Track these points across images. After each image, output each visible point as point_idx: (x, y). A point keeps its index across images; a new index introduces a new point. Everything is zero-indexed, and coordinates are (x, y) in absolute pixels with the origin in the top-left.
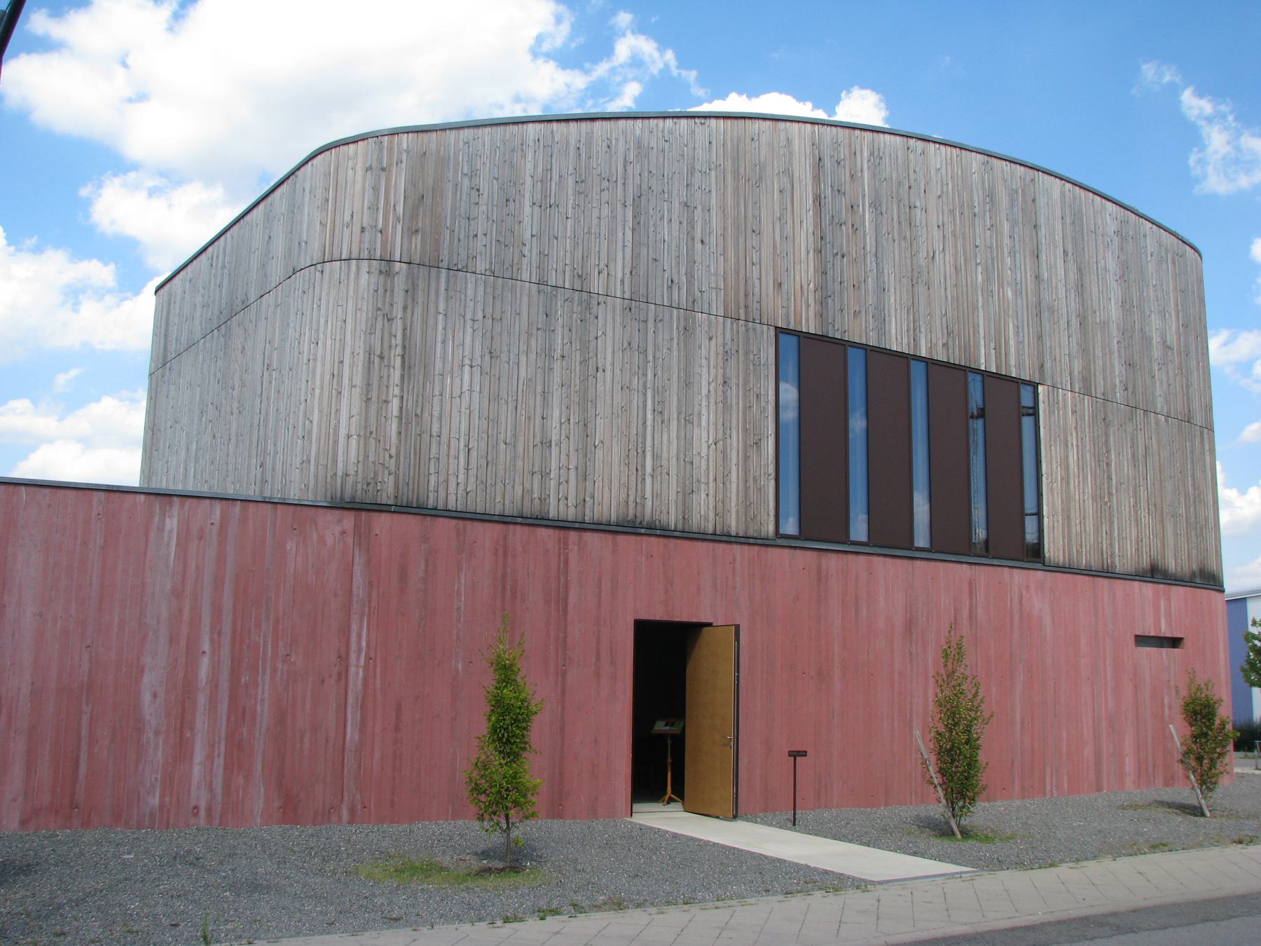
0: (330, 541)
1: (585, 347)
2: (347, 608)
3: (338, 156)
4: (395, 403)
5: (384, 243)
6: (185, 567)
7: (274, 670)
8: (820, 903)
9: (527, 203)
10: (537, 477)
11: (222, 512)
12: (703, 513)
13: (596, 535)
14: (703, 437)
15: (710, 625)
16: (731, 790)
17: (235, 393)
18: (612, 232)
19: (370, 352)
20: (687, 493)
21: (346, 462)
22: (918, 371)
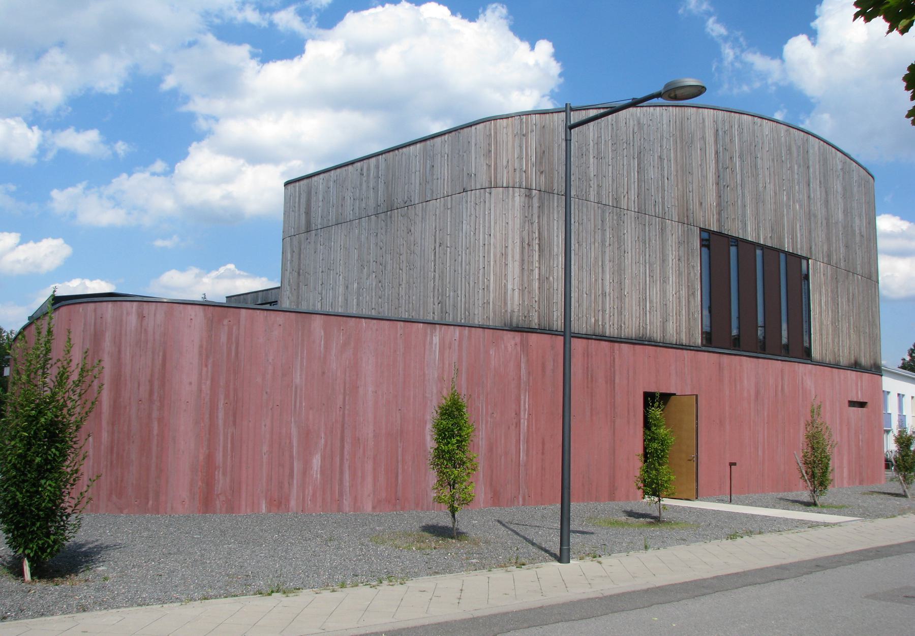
0: (510, 349)
1: (619, 238)
2: (519, 387)
3: (495, 125)
4: (537, 271)
5: (527, 178)
6: (443, 364)
7: (487, 422)
8: (823, 531)
9: (591, 157)
10: (601, 313)
11: (460, 334)
12: (672, 335)
13: (626, 345)
14: (671, 289)
15: (674, 394)
16: (695, 484)
17: (403, 258)
18: (629, 173)
19: (522, 242)
20: (665, 321)
21: (512, 304)
22: (782, 256)
